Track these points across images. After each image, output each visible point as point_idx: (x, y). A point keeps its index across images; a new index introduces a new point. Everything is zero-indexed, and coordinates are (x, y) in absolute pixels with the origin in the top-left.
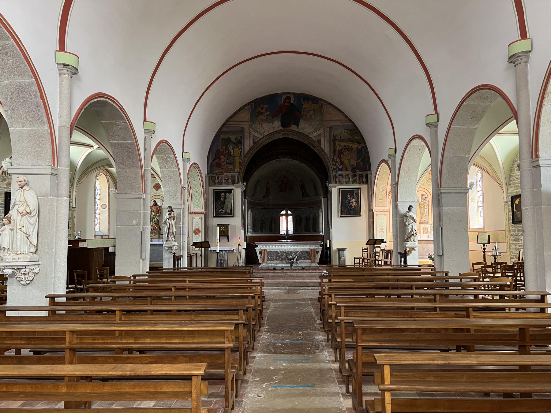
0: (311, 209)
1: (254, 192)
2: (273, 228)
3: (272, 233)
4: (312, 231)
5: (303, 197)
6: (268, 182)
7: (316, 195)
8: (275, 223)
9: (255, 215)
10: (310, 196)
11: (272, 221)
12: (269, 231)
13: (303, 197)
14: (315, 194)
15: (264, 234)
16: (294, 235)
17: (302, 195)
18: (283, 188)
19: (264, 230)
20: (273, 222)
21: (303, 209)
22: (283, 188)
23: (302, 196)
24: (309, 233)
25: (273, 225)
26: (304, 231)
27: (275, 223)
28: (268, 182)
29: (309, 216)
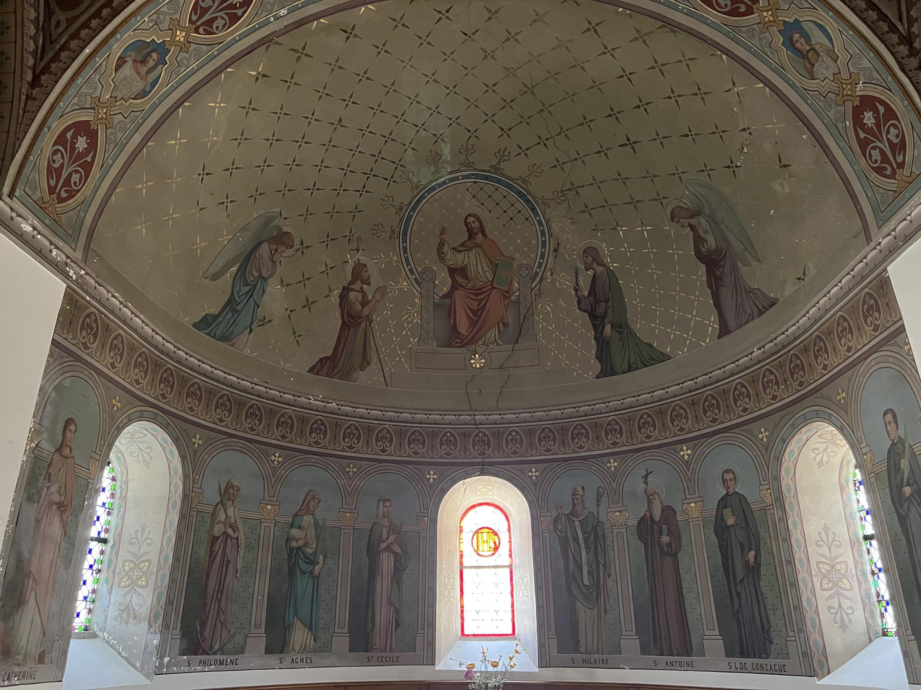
0: (686, 452)
1: (231, 304)
2: (382, 614)
3: (369, 663)
4: (714, 642)
5: (607, 370)
6: (359, 273)
7: (724, 331)
8: (398, 571)
9: (228, 494)
10: (663, 358)
11: (373, 553)
12: (342, 642)
13: (607, 370)
14: (713, 324)
15: (294, 664)
16: (551, 675)
17: (599, 357)
18: (463, 326)
19: (300, 636)
20: (386, 562)
21: (613, 464)
22: (463, 326)
23: (598, 367)
24: (690, 666)
25: (383, 586)
26: (631, 643)
27: (398, 571)
28: (359, 273)
29: (667, 511)
